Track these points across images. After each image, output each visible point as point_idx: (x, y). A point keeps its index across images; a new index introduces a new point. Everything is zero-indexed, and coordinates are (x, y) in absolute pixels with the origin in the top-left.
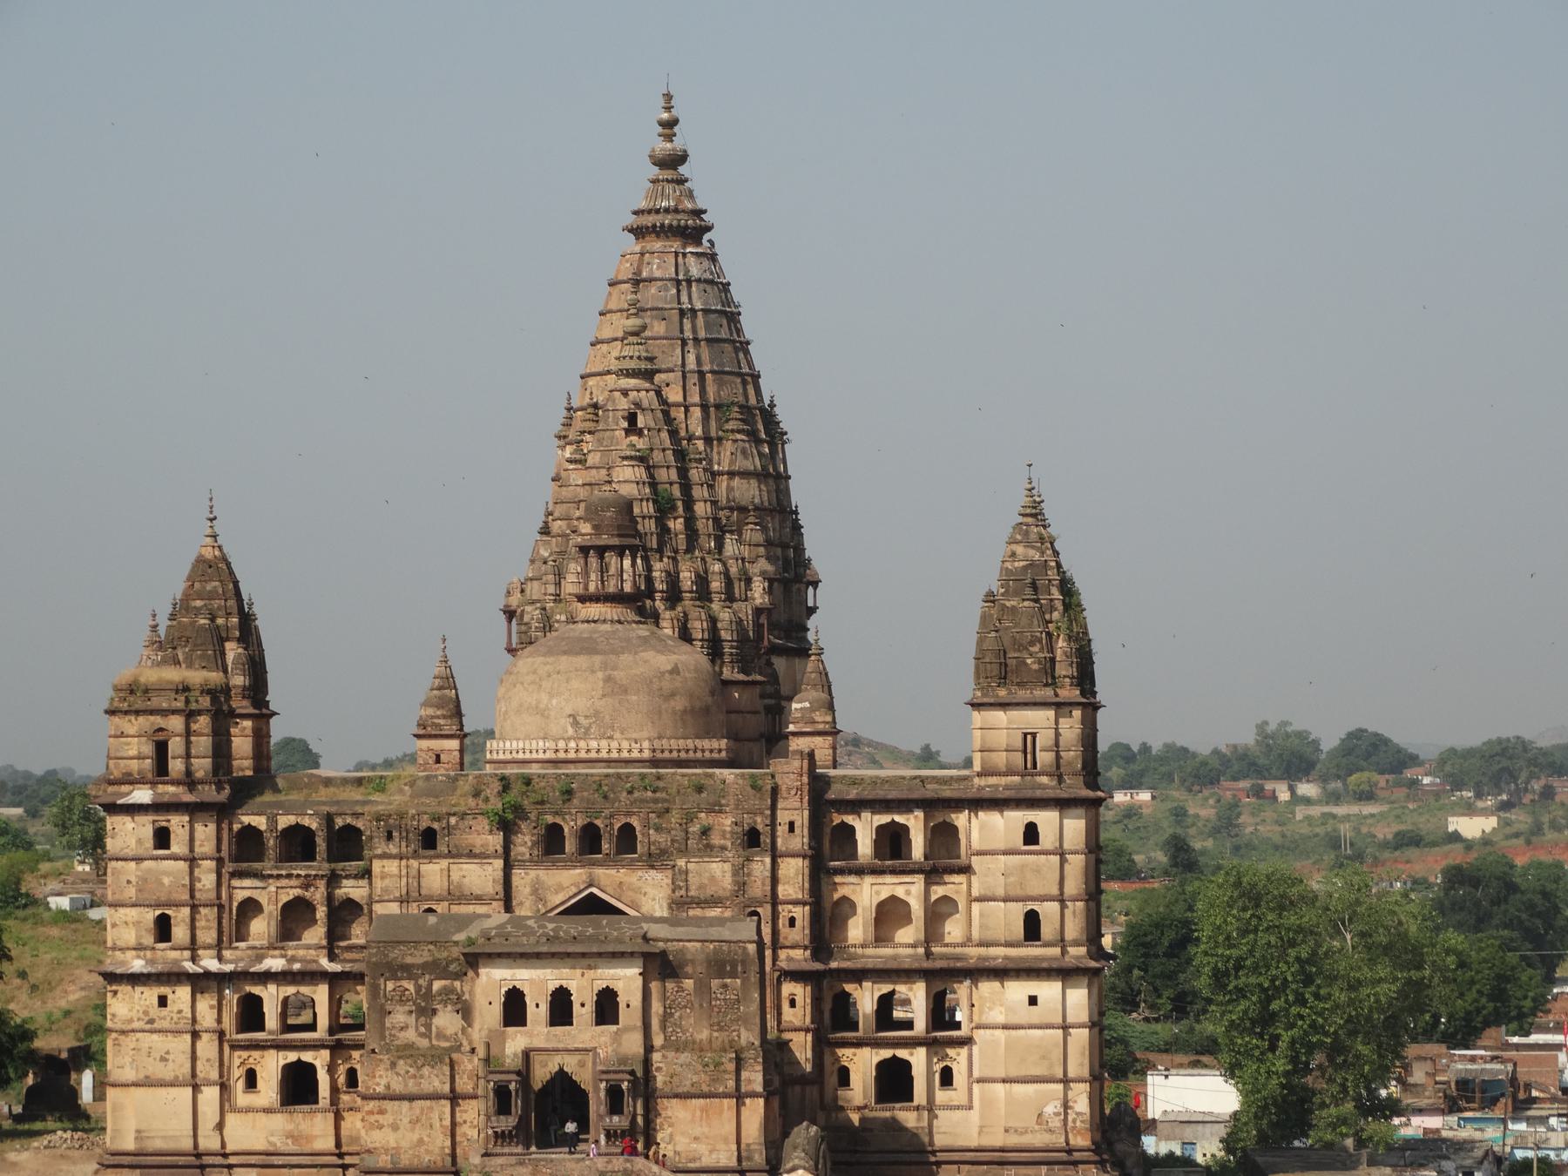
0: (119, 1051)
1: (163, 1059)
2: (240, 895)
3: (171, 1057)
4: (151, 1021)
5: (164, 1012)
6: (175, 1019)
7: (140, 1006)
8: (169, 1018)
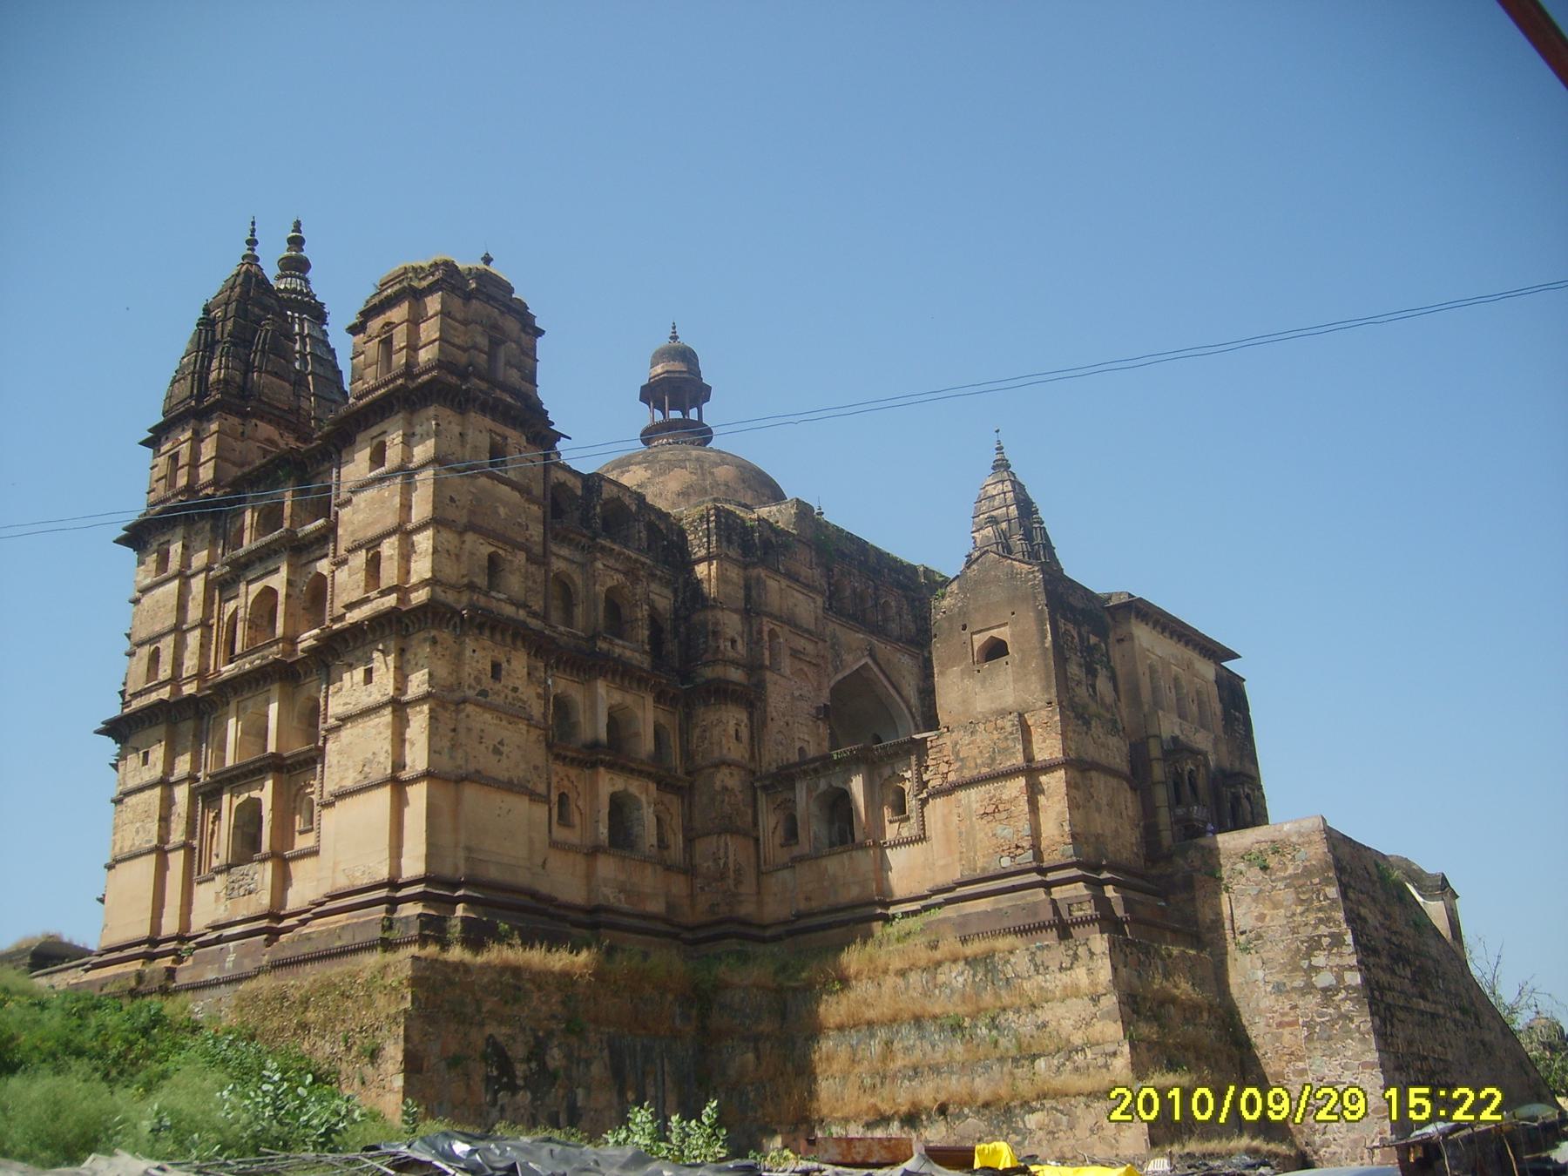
0: (437, 728)
1: (497, 751)
2: (558, 565)
3: (505, 749)
4: (484, 693)
5: (498, 686)
6: (510, 699)
7: (472, 668)
8: (503, 695)
